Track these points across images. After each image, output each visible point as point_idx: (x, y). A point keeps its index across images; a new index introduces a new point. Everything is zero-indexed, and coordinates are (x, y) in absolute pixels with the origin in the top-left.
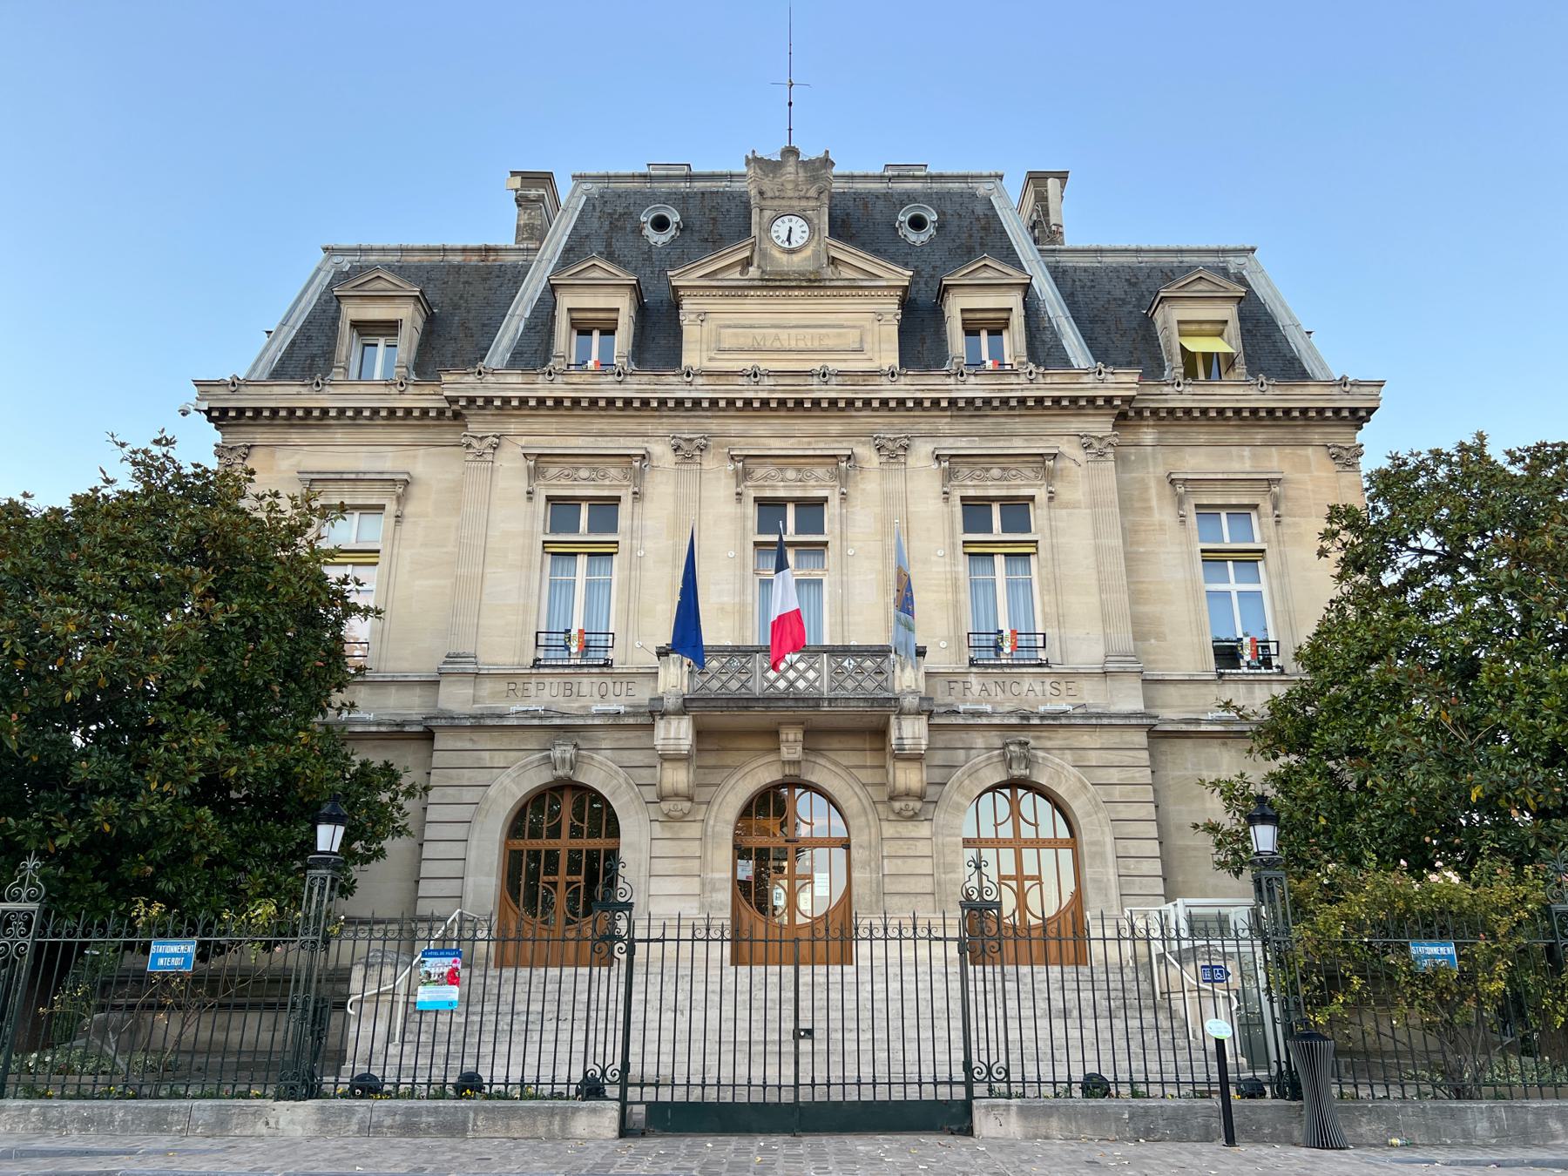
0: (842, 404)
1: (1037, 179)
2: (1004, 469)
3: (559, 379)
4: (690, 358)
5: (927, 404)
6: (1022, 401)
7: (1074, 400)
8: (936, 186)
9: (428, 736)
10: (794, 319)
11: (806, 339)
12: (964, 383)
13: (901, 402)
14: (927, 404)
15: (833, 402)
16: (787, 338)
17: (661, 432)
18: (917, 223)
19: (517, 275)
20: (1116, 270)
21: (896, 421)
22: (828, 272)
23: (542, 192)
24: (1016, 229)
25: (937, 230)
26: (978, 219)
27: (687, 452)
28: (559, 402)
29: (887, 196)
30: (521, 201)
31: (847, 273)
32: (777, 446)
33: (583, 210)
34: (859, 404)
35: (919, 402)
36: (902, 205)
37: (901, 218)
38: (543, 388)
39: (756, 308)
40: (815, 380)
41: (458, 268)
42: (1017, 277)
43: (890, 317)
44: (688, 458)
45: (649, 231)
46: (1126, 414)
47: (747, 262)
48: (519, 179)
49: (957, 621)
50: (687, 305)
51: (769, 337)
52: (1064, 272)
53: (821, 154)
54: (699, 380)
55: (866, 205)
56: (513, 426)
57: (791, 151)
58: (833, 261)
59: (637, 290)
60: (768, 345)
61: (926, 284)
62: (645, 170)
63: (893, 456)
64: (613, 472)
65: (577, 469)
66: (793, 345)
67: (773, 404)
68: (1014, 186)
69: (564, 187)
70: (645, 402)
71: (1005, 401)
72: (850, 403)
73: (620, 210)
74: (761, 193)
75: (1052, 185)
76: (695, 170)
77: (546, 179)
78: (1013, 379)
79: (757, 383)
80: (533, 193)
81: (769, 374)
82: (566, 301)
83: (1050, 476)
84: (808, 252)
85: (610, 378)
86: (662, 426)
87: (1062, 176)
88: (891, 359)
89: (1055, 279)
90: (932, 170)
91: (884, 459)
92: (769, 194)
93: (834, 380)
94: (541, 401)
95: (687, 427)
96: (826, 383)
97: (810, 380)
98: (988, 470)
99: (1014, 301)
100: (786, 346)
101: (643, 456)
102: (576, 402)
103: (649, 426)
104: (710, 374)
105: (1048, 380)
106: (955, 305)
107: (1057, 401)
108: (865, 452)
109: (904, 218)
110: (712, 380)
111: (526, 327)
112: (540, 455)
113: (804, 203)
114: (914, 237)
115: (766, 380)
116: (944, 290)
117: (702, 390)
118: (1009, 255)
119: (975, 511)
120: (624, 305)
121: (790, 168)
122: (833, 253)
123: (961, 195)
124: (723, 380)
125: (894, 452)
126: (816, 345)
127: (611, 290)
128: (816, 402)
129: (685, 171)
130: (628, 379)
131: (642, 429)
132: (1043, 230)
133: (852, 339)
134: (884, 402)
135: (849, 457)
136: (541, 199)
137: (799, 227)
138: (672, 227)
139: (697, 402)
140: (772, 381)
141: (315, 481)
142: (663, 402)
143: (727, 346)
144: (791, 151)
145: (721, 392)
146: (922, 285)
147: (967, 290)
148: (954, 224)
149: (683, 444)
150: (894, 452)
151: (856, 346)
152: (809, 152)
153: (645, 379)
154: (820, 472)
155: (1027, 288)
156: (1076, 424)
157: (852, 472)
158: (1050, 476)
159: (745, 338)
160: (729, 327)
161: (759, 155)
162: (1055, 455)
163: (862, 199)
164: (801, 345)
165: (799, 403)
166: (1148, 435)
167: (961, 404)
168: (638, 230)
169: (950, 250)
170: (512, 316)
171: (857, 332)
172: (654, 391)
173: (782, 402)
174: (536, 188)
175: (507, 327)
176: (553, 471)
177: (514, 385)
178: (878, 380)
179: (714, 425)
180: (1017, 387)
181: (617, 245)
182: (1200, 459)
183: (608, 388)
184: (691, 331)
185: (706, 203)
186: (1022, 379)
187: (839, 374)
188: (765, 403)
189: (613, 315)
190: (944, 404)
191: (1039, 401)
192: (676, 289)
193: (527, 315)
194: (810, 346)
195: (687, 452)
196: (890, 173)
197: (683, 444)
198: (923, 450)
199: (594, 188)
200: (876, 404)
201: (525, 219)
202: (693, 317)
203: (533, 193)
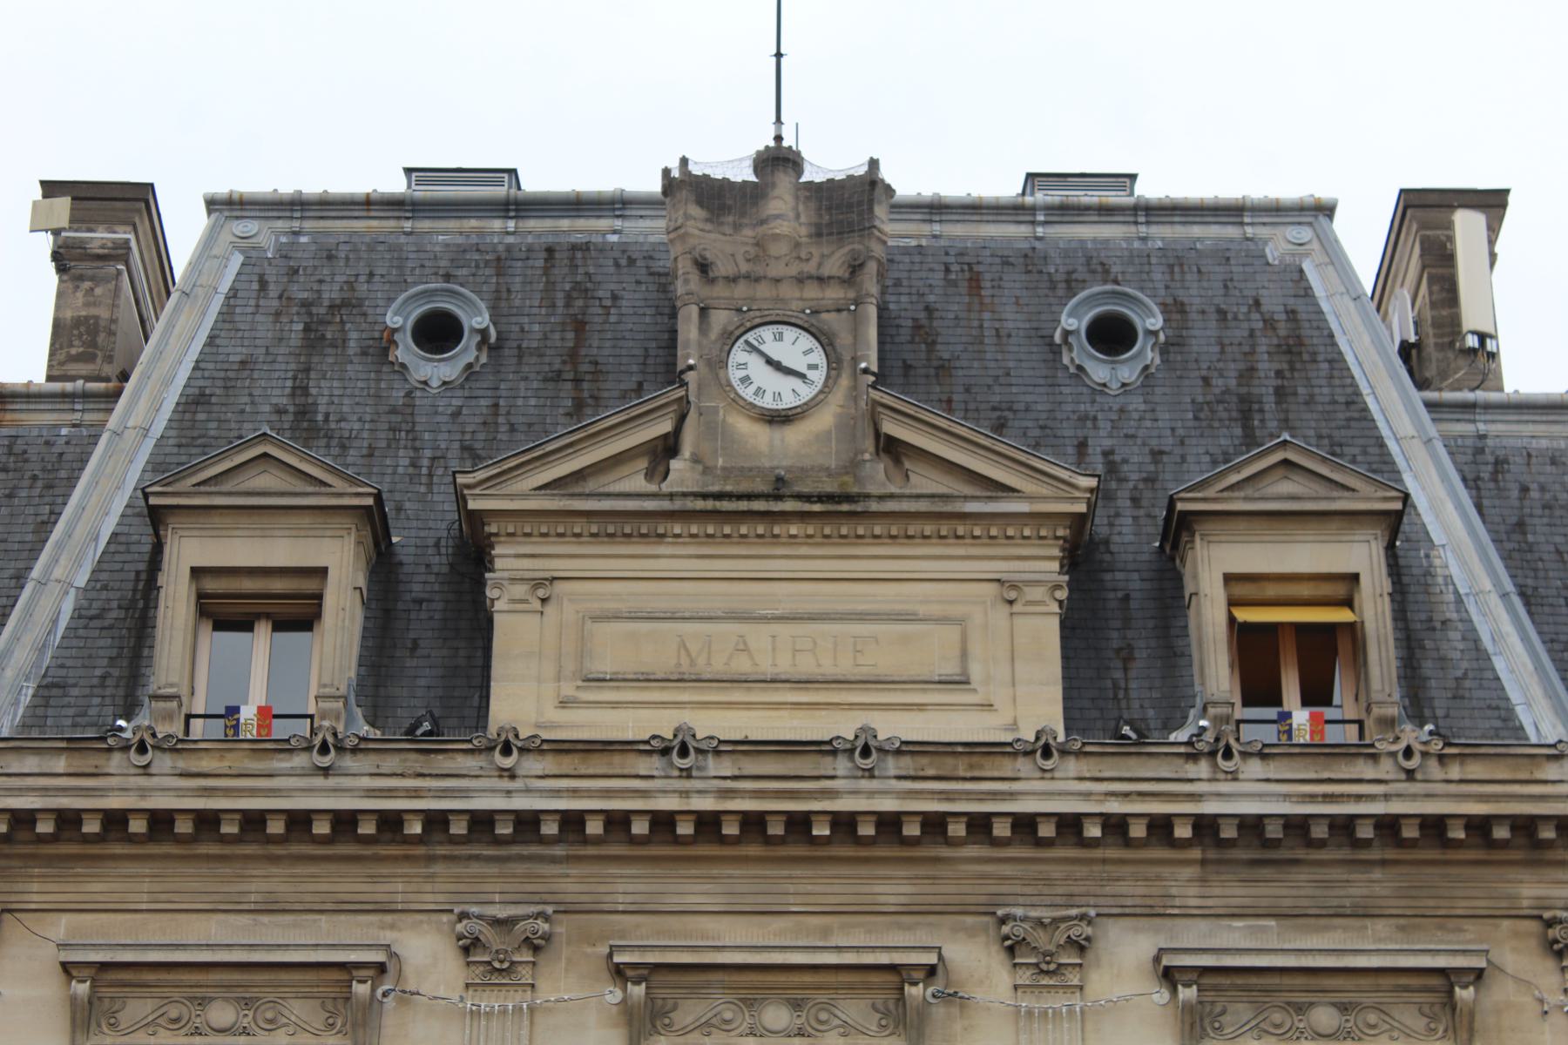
0: (912, 830)
1: (1426, 217)
2: (1344, 1008)
3: (164, 763)
4: (517, 701)
5: (1138, 831)
6: (1388, 826)
7: (1525, 826)
8: (1162, 233)
10: (784, 596)
11: (822, 649)
12: (1234, 776)
13: (1070, 825)
14: (1138, 831)
15: (889, 824)
16: (770, 649)
17: (430, 900)
18: (1112, 335)
19: (55, 472)
21: (1056, 871)
22: (877, 476)
23: (123, 234)
24: (1368, 353)
25: (1164, 350)
26: (1270, 323)
27: (498, 956)
28: (161, 822)
29: (1030, 260)
30: (61, 259)
31: (925, 481)
32: (738, 939)
33: (233, 293)
34: (957, 829)
35: (1116, 826)
36: (1072, 285)
37: (1068, 322)
38: (123, 787)
39: (683, 572)
40: (842, 765)
42: (1371, 499)
43: (1038, 593)
44: (499, 973)
45: (405, 350)
47: (668, 447)
48: (63, 204)
50: (507, 559)
51: (719, 647)
52: (1500, 464)
53: (862, 171)
54: (533, 765)
55: (975, 283)
56: (36, 889)
57: (778, 160)
58: (891, 448)
59: (375, 521)
60: (718, 666)
61: (1136, 501)
62: (397, 185)
63: (1048, 970)
64: (299, 1009)
65: (203, 1002)
66: (784, 665)
67: (731, 829)
68: (1363, 238)
69: (184, 230)
70: (391, 823)
71: (1344, 827)
72: (935, 824)
73: (331, 293)
74: (703, 267)
75: (1467, 225)
76: (532, 184)
77: (133, 201)
78: (1369, 771)
79: (687, 774)
80: (100, 237)
81: (721, 748)
82: (188, 550)
84: (824, 419)
85: (300, 761)
86: (437, 884)
87: (1492, 203)
88: (1038, 705)
89: (1472, 483)
90: (1149, 189)
91: (1025, 977)
92: (722, 268)
93: (892, 766)
94: (115, 821)
95: (497, 890)
96: (870, 774)
97: (826, 765)
98: (1300, 1009)
99: (1360, 555)
100: (766, 668)
101: (381, 968)
102: (207, 821)
103: (397, 885)
104: (563, 748)
105: (1455, 772)
106: (1212, 564)
107: (1479, 827)
108: (974, 959)
109: (1074, 320)
110: (568, 764)
111: (78, 614)
112: (104, 966)
113: (812, 291)
114: (1099, 370)
115: (714, 766)
116: (1179, 529)
117: (539, 791)
118: (1352, 434)
120: (340, 559)
121: (781, 202)
122: (891, 427)
123: (1223, 255)
124: (597, 764)
125: (1049, 957)
126: (845, 666)
127: (305, 520)
128: (844, 823)
129: (500, 192)
130: (349, 762)
131: (380, 891)
132: (1446, 351)
133: (933, 651)
134: (1025, 825)
135: (931, 971)
136: (120, 253)
137: (796, 348)
138: (469, 342)
139: (527, 823)
140: (726, 767)
142: (436, 821)
143: (605, 666)
144: (778, 160)
145: (591, 795)
146: (1124, 502)
147: (1241, 524)
148: (1203, 337)
149: (488, 934)
150: (1049, 957)
151: (950, 669)
152: (827, 159)
153: (391, 763)
154: (854, 1009)
155: (1394, 523)
156: (1529, 888)
157: (939, 1011)
159: (656, 648)
160: (616, 617)
161: (696, 170)
162: (1479, 974)
163: (970, 273)
164: (806, 666)
165: (799, 824)
167: (1228, 832)
168: (382, 347)
169: (1197, 407)
170: (41, 583)
171: (951, 634)
172: (415, 793)
173: (754, 823)
174: (111, 223)
175: (29, 612)
176: (138, 1008)
178: (1007, 767)
179: (571, 882)
180: (1375, 792)
181: (323, 392)
183: (295, 788)
184: (518, 634)
185: (560, 271)
186: (1386, 769)
187: (908, 749)
188: (708, 823)
189: (308, 585)
190: (1183, 831)
191: (1434, 826)
192: (476, 519)
193: (82, 580)
194: (828, 668)
195: (498, 956)
196: (1040, 197)
197: (488, 934)
198: (1127, 952)
199: (265, 234)
200: (1001, 829)
201: (78, 306)
202: (520, 590)
203: (100, 237)
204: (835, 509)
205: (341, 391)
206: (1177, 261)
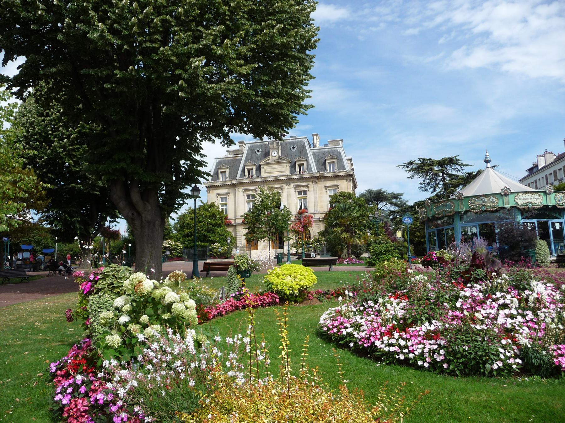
4: (263, 174)
9: (236, 226)
11: (278, 170)
16: (275, 170)
20: (322, 152)
29: (290, 142)
41: (232, 160)
46: (318, 178)
49: (296, 208)
51: (272, 170)
75: (315, 137)
83: (308, 187)
117: (264, 179)
119: (300, 193)
141: (219, 195)
145: (266, 179)
158: (308, 187)
159: (269, 171)
166: (323, 180)
177: (241, 181)
182: (329, 183)
184: (263, 170)
204: (278, 163)
205: (254, 155)
206: (298, 142)
